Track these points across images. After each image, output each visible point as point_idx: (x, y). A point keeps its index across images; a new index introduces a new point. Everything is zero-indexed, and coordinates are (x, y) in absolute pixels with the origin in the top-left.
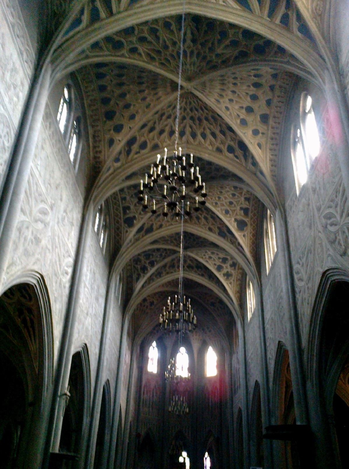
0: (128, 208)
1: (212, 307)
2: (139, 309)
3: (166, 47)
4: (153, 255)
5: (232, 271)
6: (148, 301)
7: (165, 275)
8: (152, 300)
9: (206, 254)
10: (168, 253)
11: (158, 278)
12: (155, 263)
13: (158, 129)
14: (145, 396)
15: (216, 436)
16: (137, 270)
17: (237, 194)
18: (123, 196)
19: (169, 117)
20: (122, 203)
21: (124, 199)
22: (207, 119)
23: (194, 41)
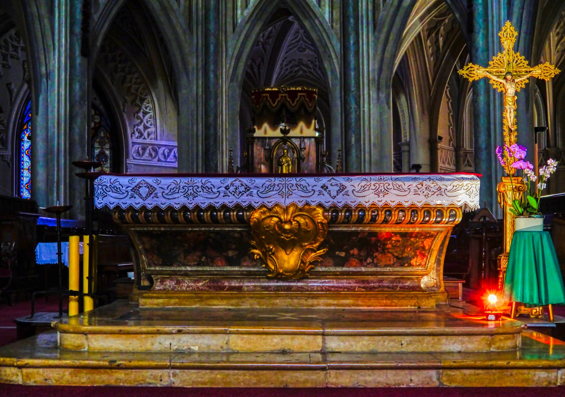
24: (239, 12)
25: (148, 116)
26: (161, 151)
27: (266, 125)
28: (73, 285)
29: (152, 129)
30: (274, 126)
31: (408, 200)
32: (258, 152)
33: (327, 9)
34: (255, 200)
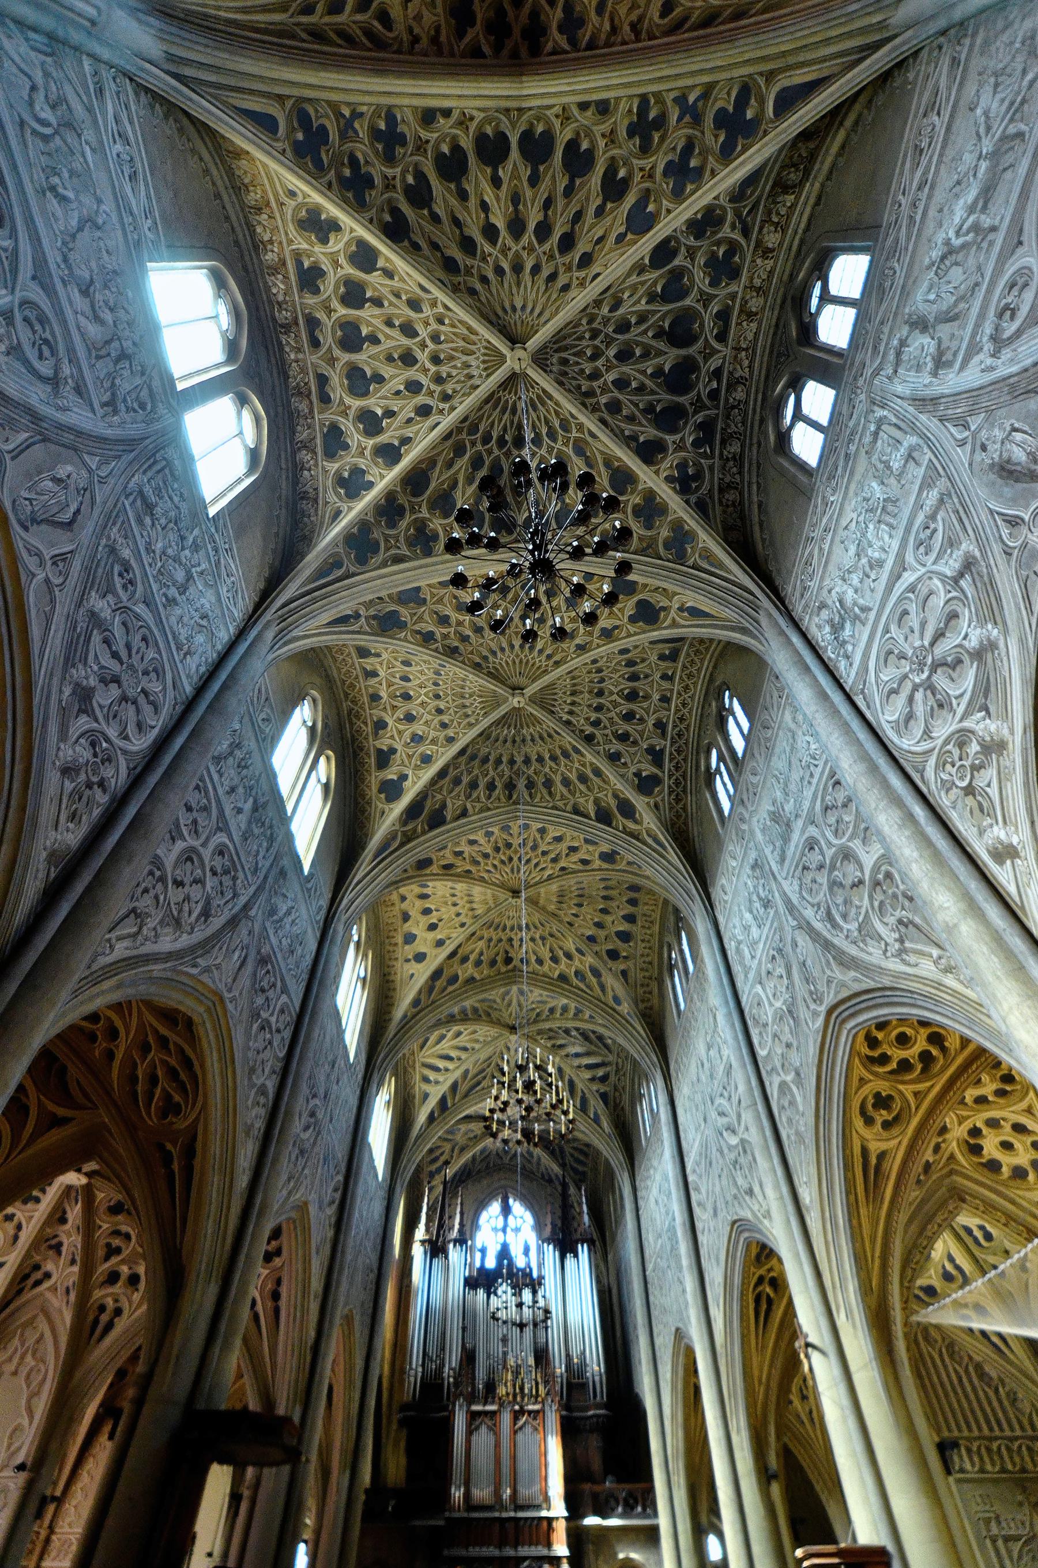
0: (662, 657)
3: (543, 938)
4: (652, 298)
5: (305, 246)
7: (618, 99)
9: (434, 326)
10: (584, 322)
11: (657, 95)
12: (647, 261)
13: (563, 847)
16: (738, 214)
17: (398, 681)
18: (666, 685)
19: (544, 853)
20: (669, 717)
21: (665, 677)
22: (486, 856)
23: (510, 940)
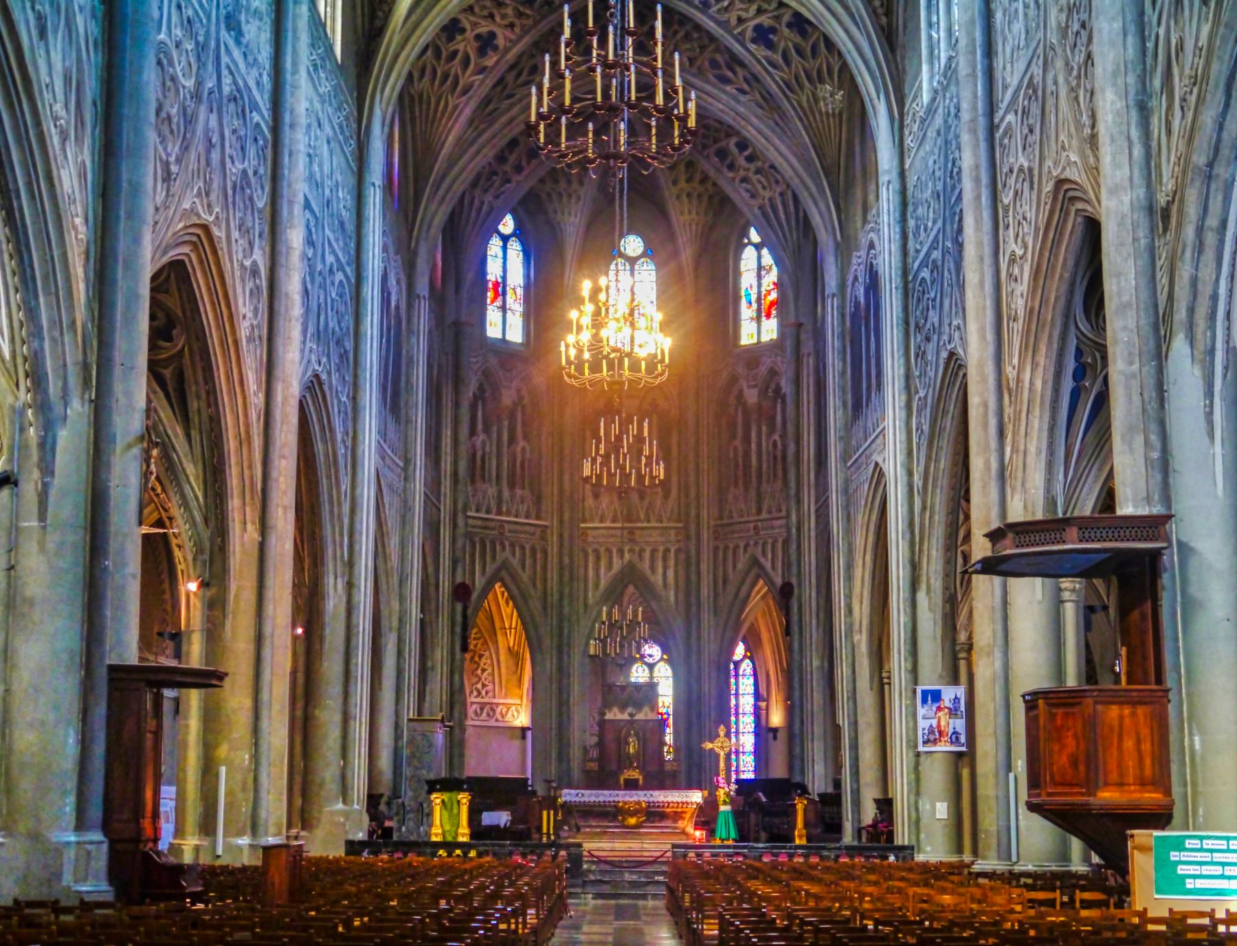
1: (761, 52)
2: (428, 71)
6: (469, 34)
8: (483, 29)
14: (482, 437)
15: (779, 581)
24: (590, 595)
25: (485, 674)
26: (498, 710)
27: (615, 710)
28: (545, 831)
29: (490, 687)
30: (623, 709)
31: (675, 800)
32: (610, 736)
33: (672, 593)
34: (620, 799)
